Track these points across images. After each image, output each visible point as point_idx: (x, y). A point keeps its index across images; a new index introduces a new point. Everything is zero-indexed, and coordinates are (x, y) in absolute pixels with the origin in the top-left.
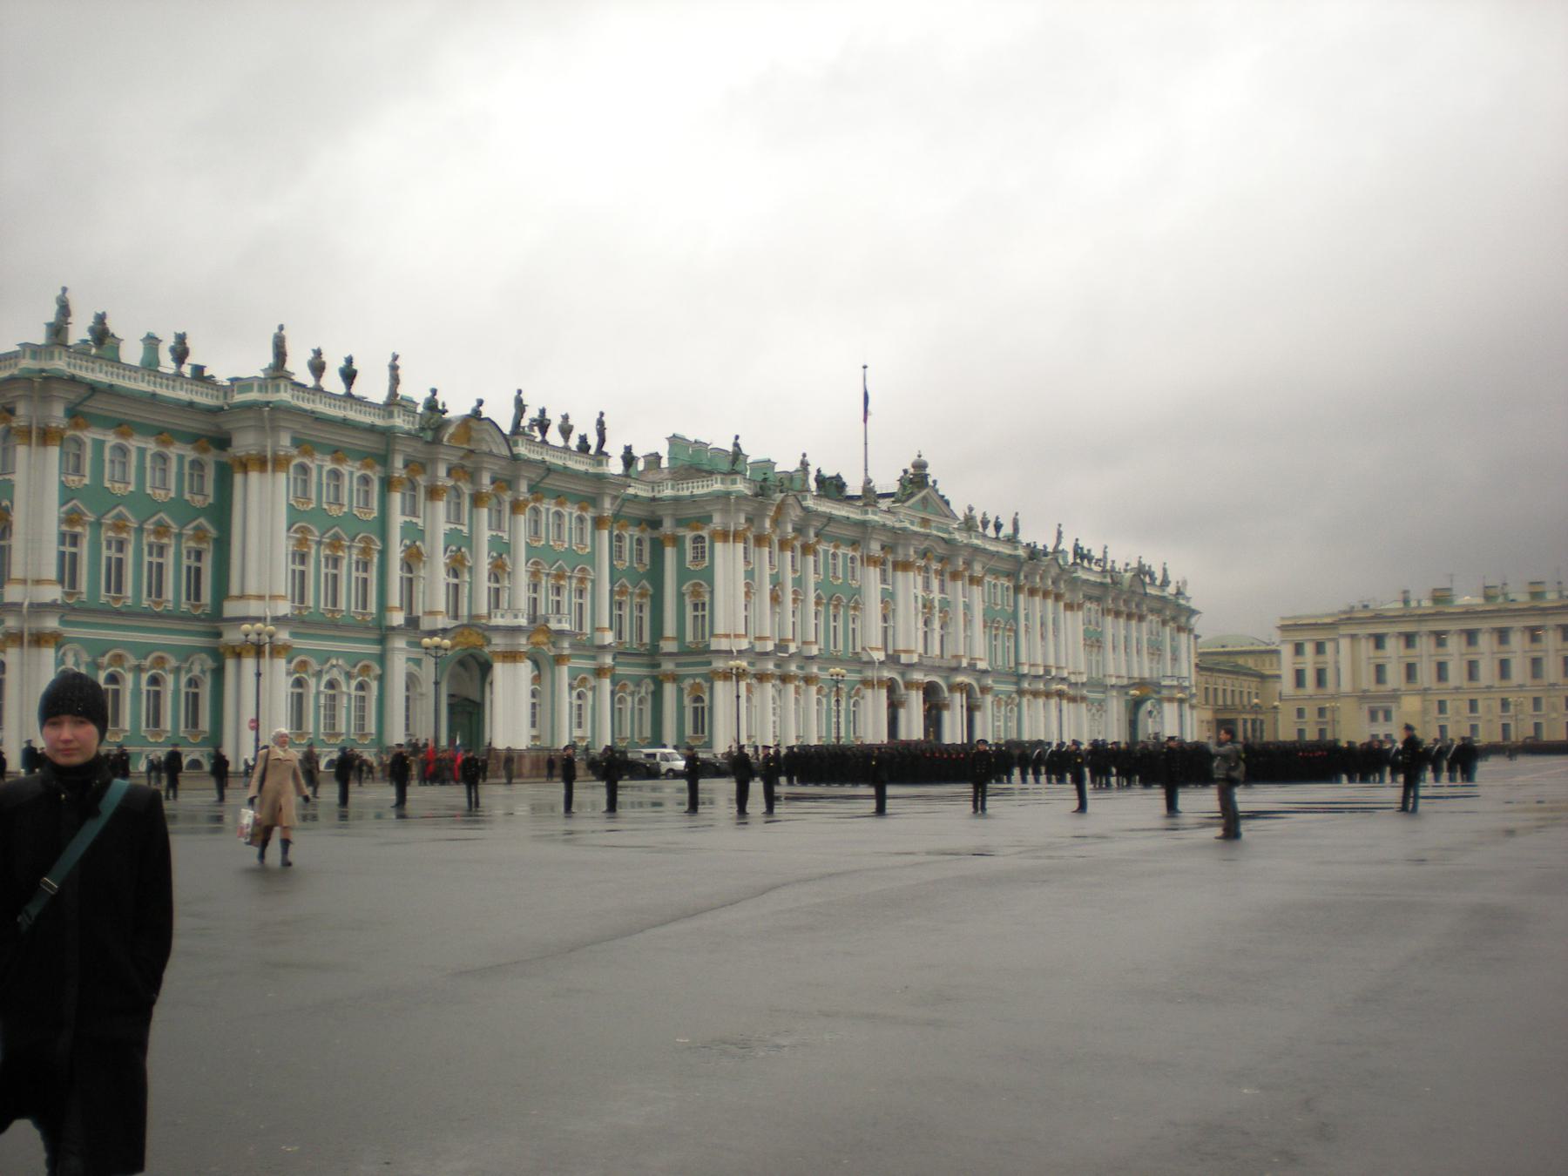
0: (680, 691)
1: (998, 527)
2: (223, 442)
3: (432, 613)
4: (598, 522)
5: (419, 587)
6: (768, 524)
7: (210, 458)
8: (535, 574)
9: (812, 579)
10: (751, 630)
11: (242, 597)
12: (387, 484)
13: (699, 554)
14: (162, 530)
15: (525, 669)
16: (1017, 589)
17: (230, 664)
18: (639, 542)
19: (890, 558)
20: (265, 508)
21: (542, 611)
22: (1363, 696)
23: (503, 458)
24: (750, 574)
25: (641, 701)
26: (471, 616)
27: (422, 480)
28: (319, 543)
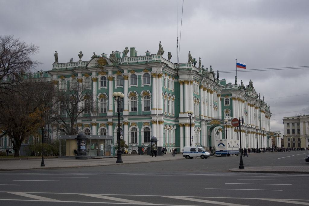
4: (218, 96)
11: (184, 112)
12: (200, 87)
13: (227, 103)
17: (181, 128)
20: (189, 91)
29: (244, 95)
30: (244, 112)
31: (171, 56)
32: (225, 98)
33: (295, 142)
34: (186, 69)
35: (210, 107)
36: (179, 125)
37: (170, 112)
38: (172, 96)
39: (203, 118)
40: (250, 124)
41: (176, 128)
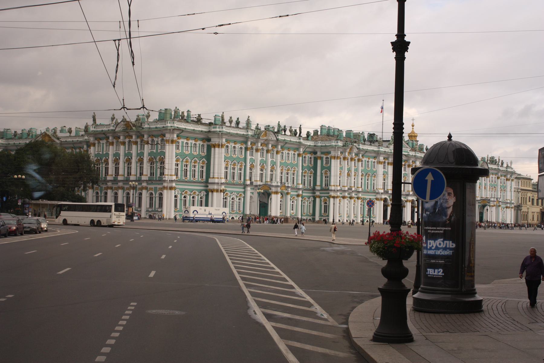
0: (321, 200)
2: (209, 140)
3: (256, 181)
4: (299, 155)
5: (253, 174)
6: (347, 154)
7: (206, 144)
8: (282, 170)
9: (360, 168)
10: (341, 184)
11: (213, 178)
12: (246, 149)
13: (327, 163)
14: (195, 162)
15: (279, 195)
17: (210, 194)
18: (311, 158)
19: (387, 161)
21: (283, 181)
24: (341, 168)
25: (310, 203)
26: (266, 182)
27: (254, 147)
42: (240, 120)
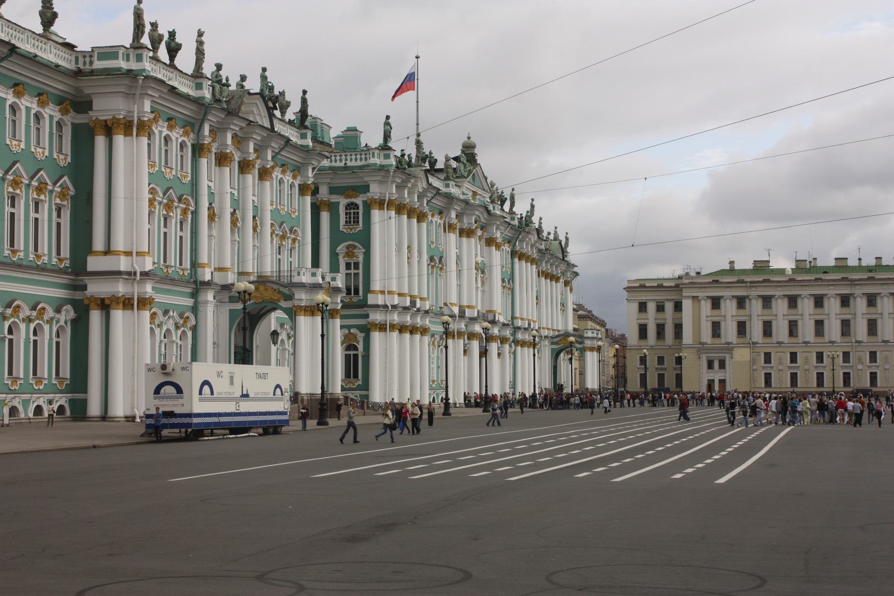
1: (503, 202)
2: (82, 105)
4: (303, 189)
11: (108, 252)
12: (198, 150)
13: (352, 219)
16: (513, 254)
20: (131, 169)
22: (701, 347)
23: (267, 129)
28: (160, 203)
29: (425, 190)
30: (425, 257)
31: (55, 15)
32: (343, 202)
33: (665, 369)
34: (119, 69)
35: (253, 228)
36: (86, 302)
37: (173, 260)
38: (164, 194)
39: (208, 277)
40: (454, 300)
41: (72, 315)
42: (178, 40)
